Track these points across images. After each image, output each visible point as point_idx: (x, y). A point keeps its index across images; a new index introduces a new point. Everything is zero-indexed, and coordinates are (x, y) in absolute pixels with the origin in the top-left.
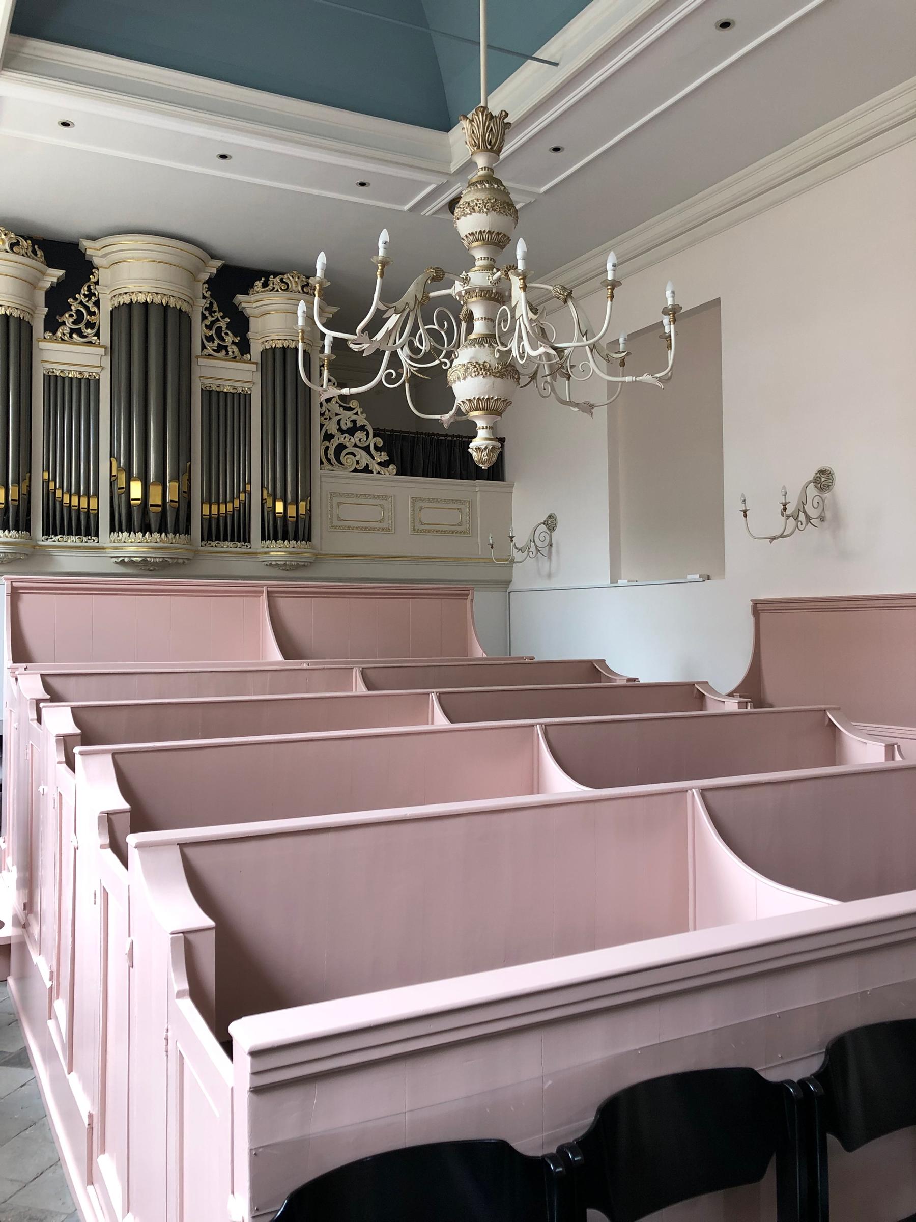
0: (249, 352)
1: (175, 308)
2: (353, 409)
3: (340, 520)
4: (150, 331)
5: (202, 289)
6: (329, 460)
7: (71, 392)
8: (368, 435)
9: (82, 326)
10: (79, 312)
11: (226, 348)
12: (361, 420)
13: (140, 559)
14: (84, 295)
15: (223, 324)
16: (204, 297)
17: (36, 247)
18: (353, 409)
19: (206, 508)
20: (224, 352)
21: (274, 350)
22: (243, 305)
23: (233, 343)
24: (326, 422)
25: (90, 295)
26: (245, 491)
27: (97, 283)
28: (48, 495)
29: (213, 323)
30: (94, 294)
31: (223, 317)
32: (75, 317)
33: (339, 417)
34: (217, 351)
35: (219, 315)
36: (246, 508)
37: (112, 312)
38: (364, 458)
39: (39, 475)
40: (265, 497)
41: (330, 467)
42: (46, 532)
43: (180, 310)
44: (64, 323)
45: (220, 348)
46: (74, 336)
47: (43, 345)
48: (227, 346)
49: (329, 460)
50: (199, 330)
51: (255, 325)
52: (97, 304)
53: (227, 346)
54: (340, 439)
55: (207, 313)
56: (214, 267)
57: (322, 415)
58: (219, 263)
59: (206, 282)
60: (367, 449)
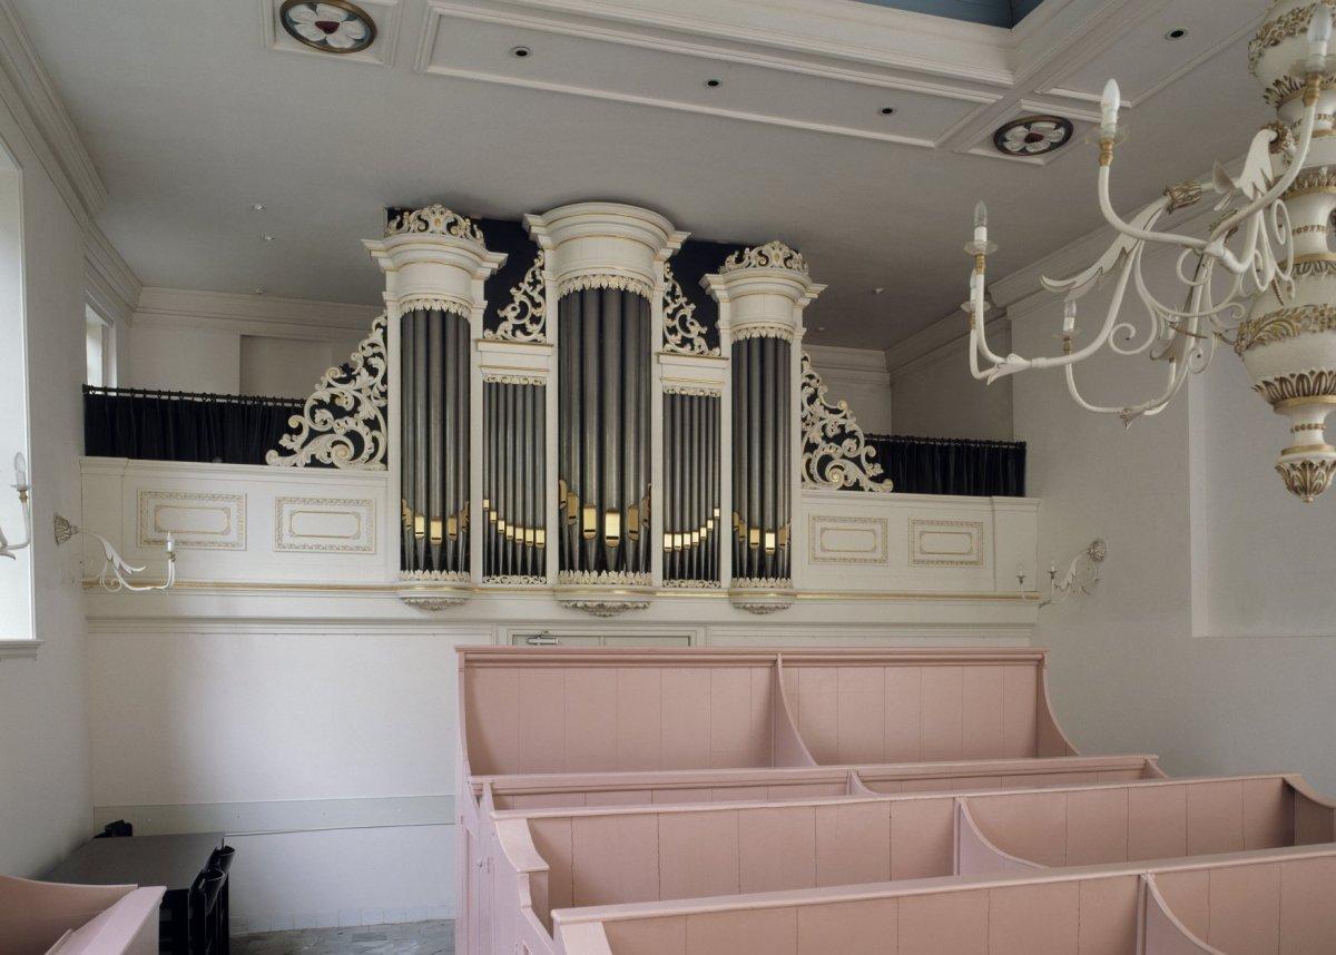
0: (717, 344)
1: (634, 293)
2: (841, 411)
3: (824, 550)
4: (602, 326)
5: (661, 269)
6: (811, 476)
7: (510, 401)
8: (858, 443)
9: (526, 321)
10: (522, 304)
11: (691, 341)
12: (851, 425)
13: (595, 604)
14: (528, 282)
15: (688, 311)
16: (666, 280)
17: (475, 226)
18: (841, 411)
19: (668, 538)
20: (689, 347)
21: (749, 341)
22: (713, 287)
23: (700, 334)
24: (808, 429)
25: (535, 283)
26: (713, 518)
27: (542, 268)
28: (489, 527)
29: (676, 311)
30: (539, 282)
31: (687, 304)
32: (519, 310)
33: (823, 422)
34: (681, 345)
35: (682, 300)
36: (715, 535)
37: (559, 302)
38: (853, 472)
39: (478, 504)
40: (736, 524)
41: (812, 485)
42: (489, 571)
43: (640, 295)
44: (505, 319)
45: (685, 341)
46: (518, 333)
47: (482, 346)
48: (692, 340)
49: (811, 476)
50: (659, 321)
51: (725, 311)
52: (542, 293)
53: (692, 340)
54: (825, 449)
55: (669, 299)
56: (677, 241)
57: (804, 420)
58: (683, 236)
59: (671, 260)
60: (857, 461)
